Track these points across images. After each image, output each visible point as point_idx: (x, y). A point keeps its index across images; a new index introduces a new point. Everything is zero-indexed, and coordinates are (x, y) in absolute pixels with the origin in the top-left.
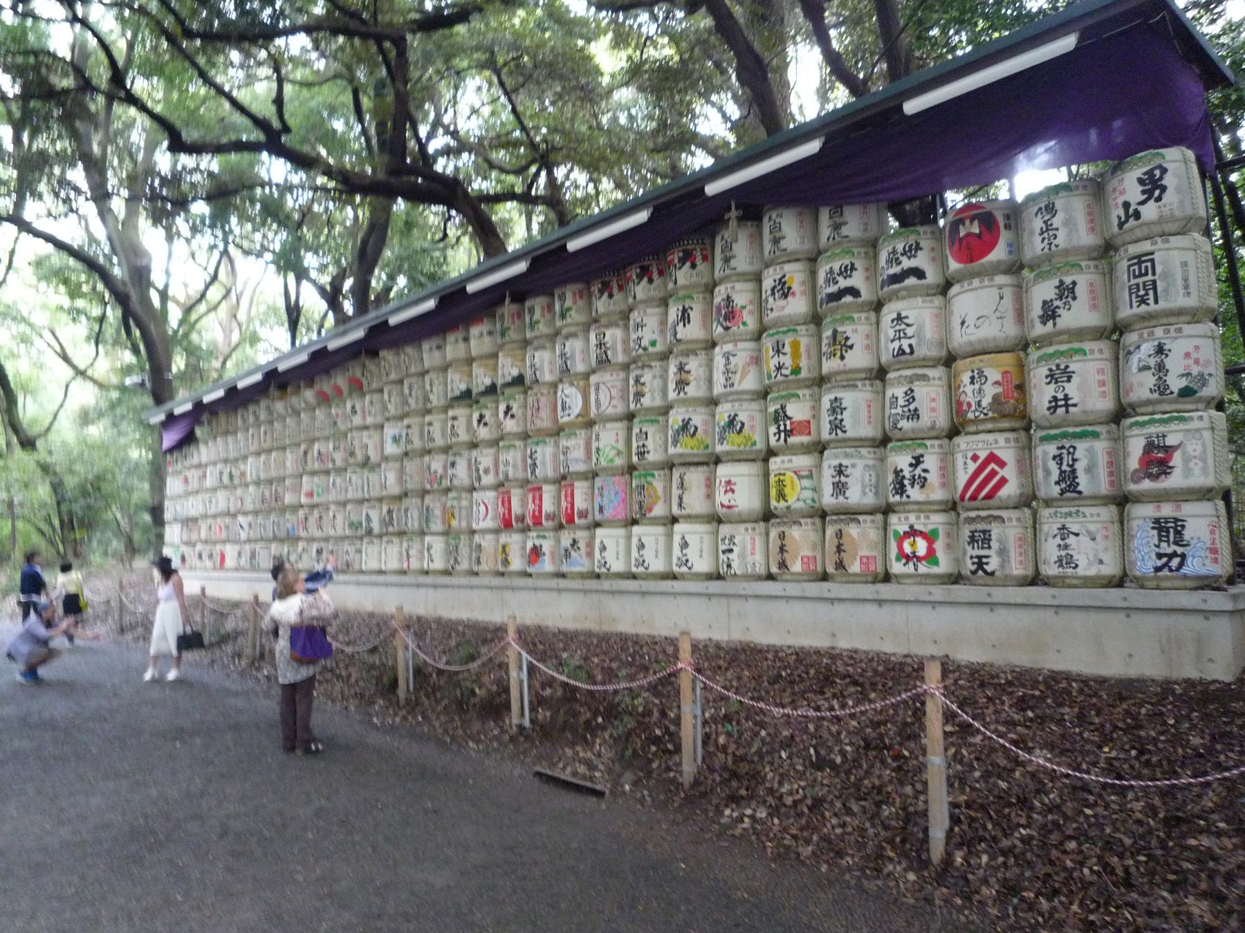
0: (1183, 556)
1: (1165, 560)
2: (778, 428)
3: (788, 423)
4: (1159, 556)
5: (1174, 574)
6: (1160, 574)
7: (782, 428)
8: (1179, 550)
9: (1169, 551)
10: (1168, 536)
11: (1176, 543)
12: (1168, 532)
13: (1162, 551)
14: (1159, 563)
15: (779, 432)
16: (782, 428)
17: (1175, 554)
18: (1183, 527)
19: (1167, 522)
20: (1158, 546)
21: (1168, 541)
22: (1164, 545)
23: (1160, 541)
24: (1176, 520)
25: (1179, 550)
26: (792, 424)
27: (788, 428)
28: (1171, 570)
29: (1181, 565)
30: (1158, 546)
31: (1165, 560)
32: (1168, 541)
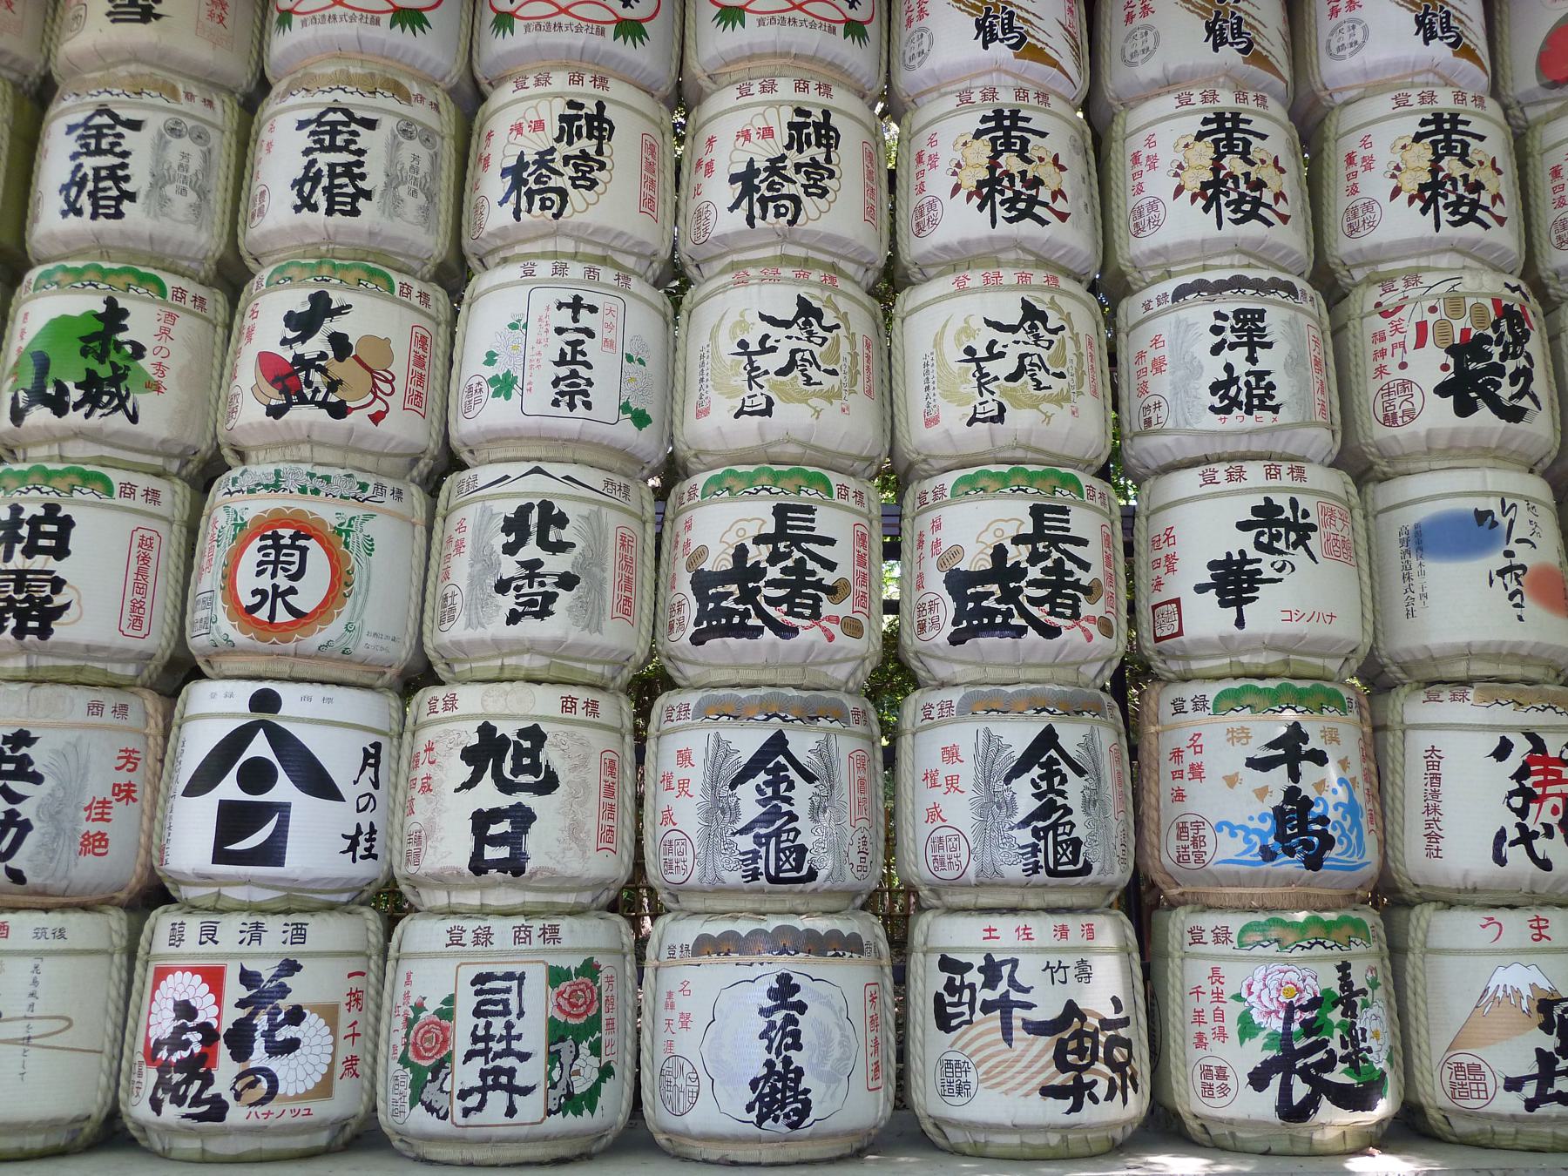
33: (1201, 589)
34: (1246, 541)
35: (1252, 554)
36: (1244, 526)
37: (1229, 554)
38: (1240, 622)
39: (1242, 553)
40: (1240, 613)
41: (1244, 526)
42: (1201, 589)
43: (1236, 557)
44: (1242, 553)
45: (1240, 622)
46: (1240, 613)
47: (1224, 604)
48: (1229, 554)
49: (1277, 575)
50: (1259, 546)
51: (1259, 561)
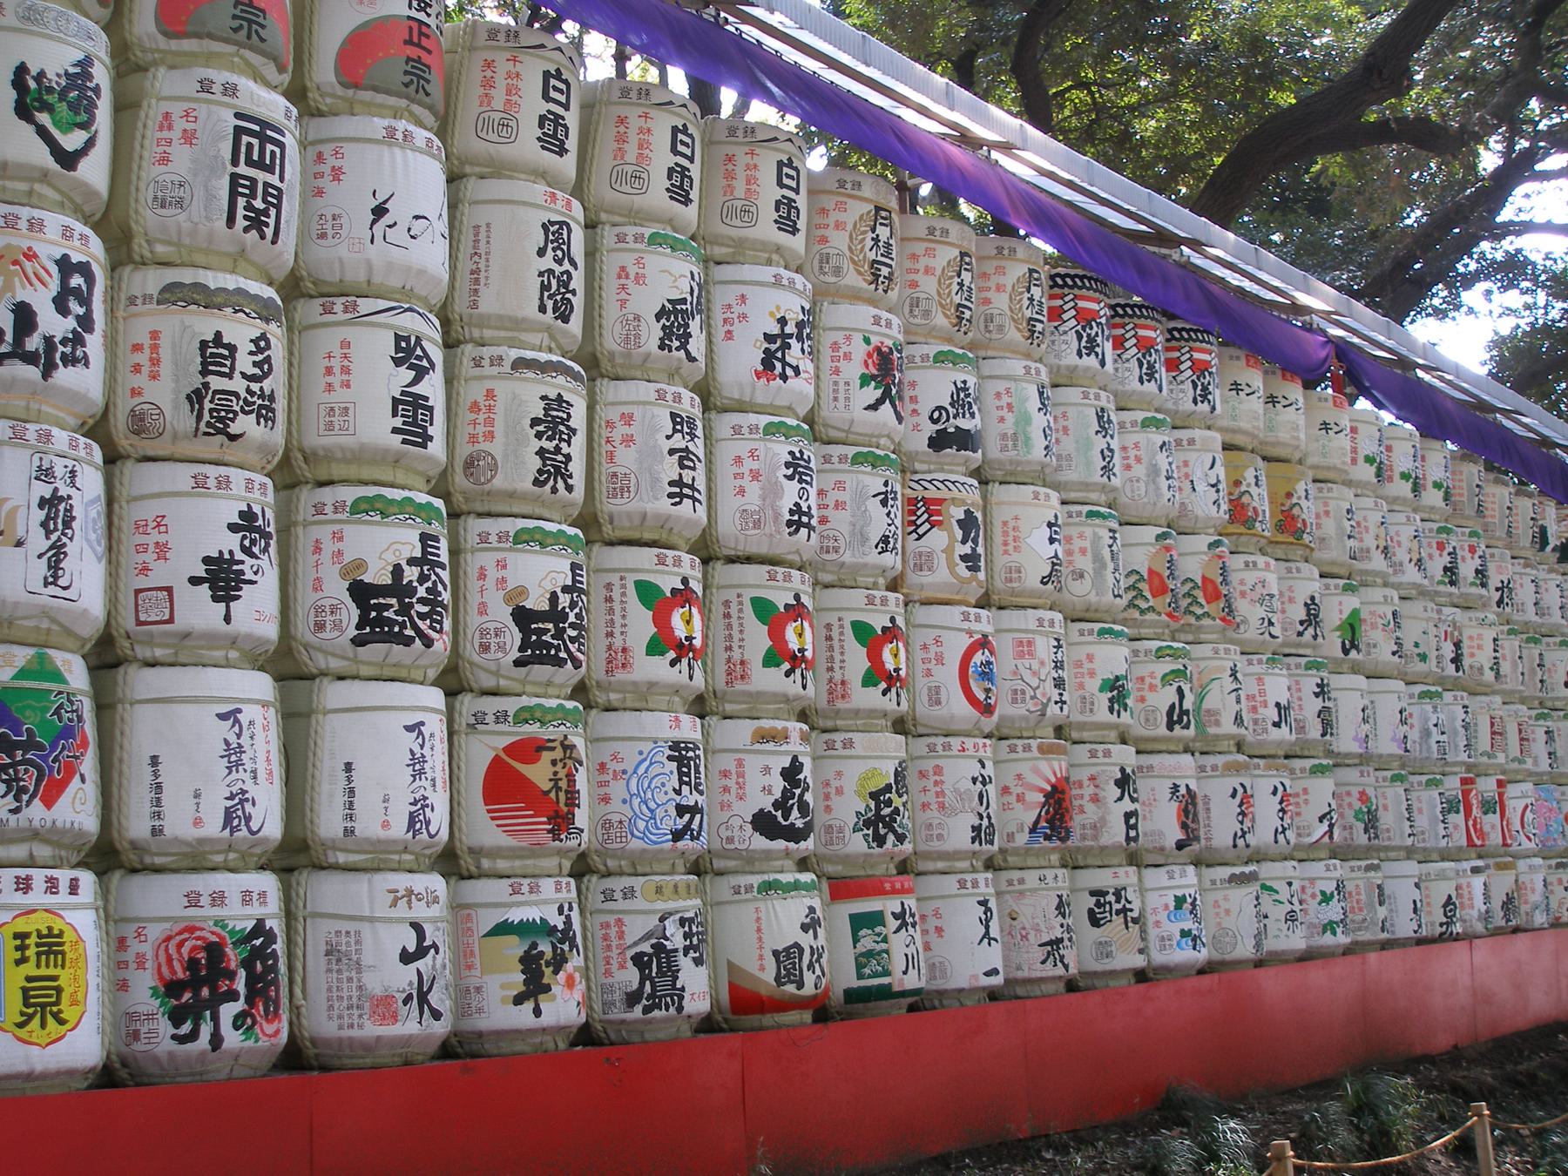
33: (195, 581)
34: (232, 542)
35: (239, 556)
36: (233, 528)
37: (221, 552)
38: (227, 619)
39: (231, 552)
40: (228, 607)
41: (233, 528)
42: (195, 581)
43: (227, 556)
44: (231, 552)
45: (227, 619)
46: (228, 607)
47: (215, 599)
48: (221, 552)
49: (254, 578)
50: (244, 549)
51: (242, 562)
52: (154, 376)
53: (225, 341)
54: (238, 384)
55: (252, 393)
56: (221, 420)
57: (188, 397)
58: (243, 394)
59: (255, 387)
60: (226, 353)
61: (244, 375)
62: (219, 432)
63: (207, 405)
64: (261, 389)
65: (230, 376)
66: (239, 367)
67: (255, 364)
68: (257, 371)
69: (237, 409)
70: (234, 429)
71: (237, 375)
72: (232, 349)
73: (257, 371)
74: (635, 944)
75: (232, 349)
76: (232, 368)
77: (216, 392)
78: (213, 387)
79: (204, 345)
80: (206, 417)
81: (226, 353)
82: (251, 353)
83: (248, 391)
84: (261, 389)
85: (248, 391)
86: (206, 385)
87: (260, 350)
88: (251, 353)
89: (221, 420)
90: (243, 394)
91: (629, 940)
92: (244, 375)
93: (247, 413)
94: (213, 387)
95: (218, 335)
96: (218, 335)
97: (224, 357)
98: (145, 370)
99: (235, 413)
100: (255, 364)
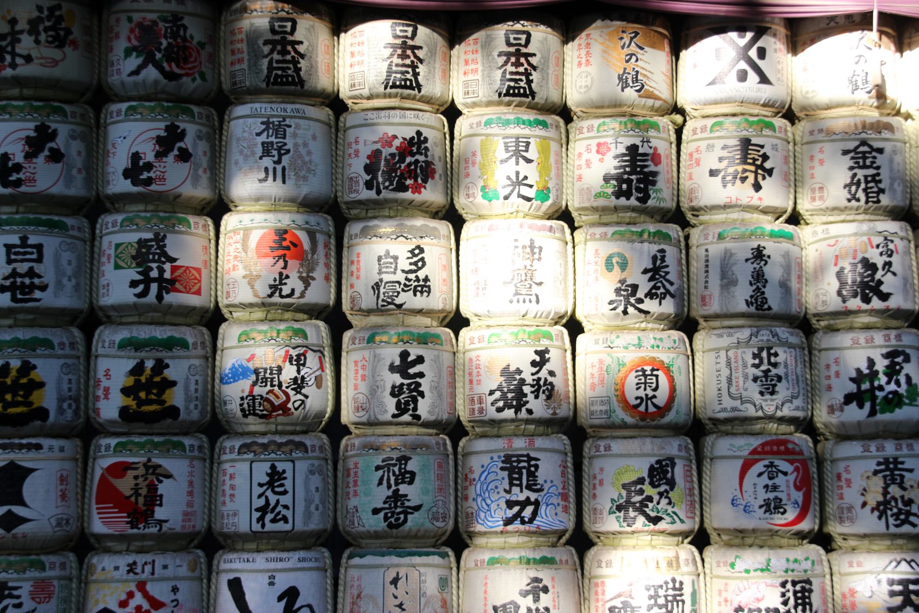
0: (537, 504)
1: (516, 509)
2: (145, 273)
3: (167, 267)
4: (510, 504)
5: (527, 527)
6: (510, 528)
7: (154, 274)
8: (533, 496)
9: (522, 497)
10: (520, 479)
11: (529, 487)
12: (521, 474)
13: (514, 498)
14: (510, 513)
15: (147, 281)
16: (154, 274)
17: (527, 502)
18: (537, 467)
19: (519, 461)
20: (508, 492)
21: (520, 485)
22: (516, 490)
23: (511, 484)
24: (530, 459)
25: (533, 496)
26: (174, 269)
27: (167, 275)
28: (523, 522)
29: (535, 514)
30: (508, 492)
31: (516, 509)
32: (520, 485)
52: (358, 278)
53: (391, 254)
54: (401, 277)
55: (409, 280)
56: (388, 297)
57: (373, 287)
58: (403, 281)
59: (412, 276)
60: (392, 260)
61: (403, 271)
62: (389, 303)
63: (382, 290)
64: (417, 277)
65: (395, 273)
66: (400, 267)
67: (411, 264)
68: (413, 267)
69: (400, 290)
70: (398, 301)
71: (399, 272)
72: (396, 258)
73: (413, 267)
74: (612, 599)
75: (396, 258)
76: (396, 269)
77: (387, 283)
78: (385, 281)
79: (380, 259)
80: (382, 296)
81: (392, 260)
82: (408, 258)
83: (407, 279)
84: (417, 277)
85: (407, 279)
86: (381, 280)
87: (415, 255)
88: (408, 258)
89: (388, 297)
90: (403, 281)
91: (607, 597)
92: (403, 271)
93: (405, 291)
94: (385, 281)
95: (388, 252)
96: (388, 252)
97: (391, 263)
98: (355, 274)
99: (399, 293)
100: (411, 264)
